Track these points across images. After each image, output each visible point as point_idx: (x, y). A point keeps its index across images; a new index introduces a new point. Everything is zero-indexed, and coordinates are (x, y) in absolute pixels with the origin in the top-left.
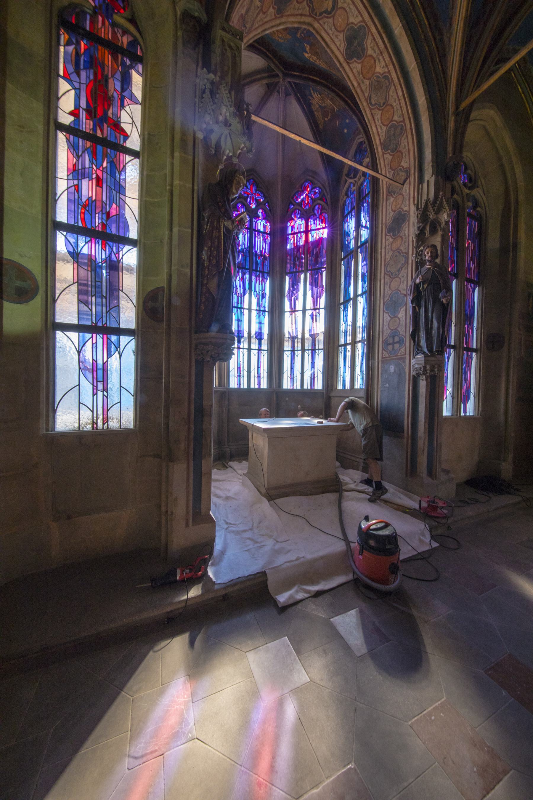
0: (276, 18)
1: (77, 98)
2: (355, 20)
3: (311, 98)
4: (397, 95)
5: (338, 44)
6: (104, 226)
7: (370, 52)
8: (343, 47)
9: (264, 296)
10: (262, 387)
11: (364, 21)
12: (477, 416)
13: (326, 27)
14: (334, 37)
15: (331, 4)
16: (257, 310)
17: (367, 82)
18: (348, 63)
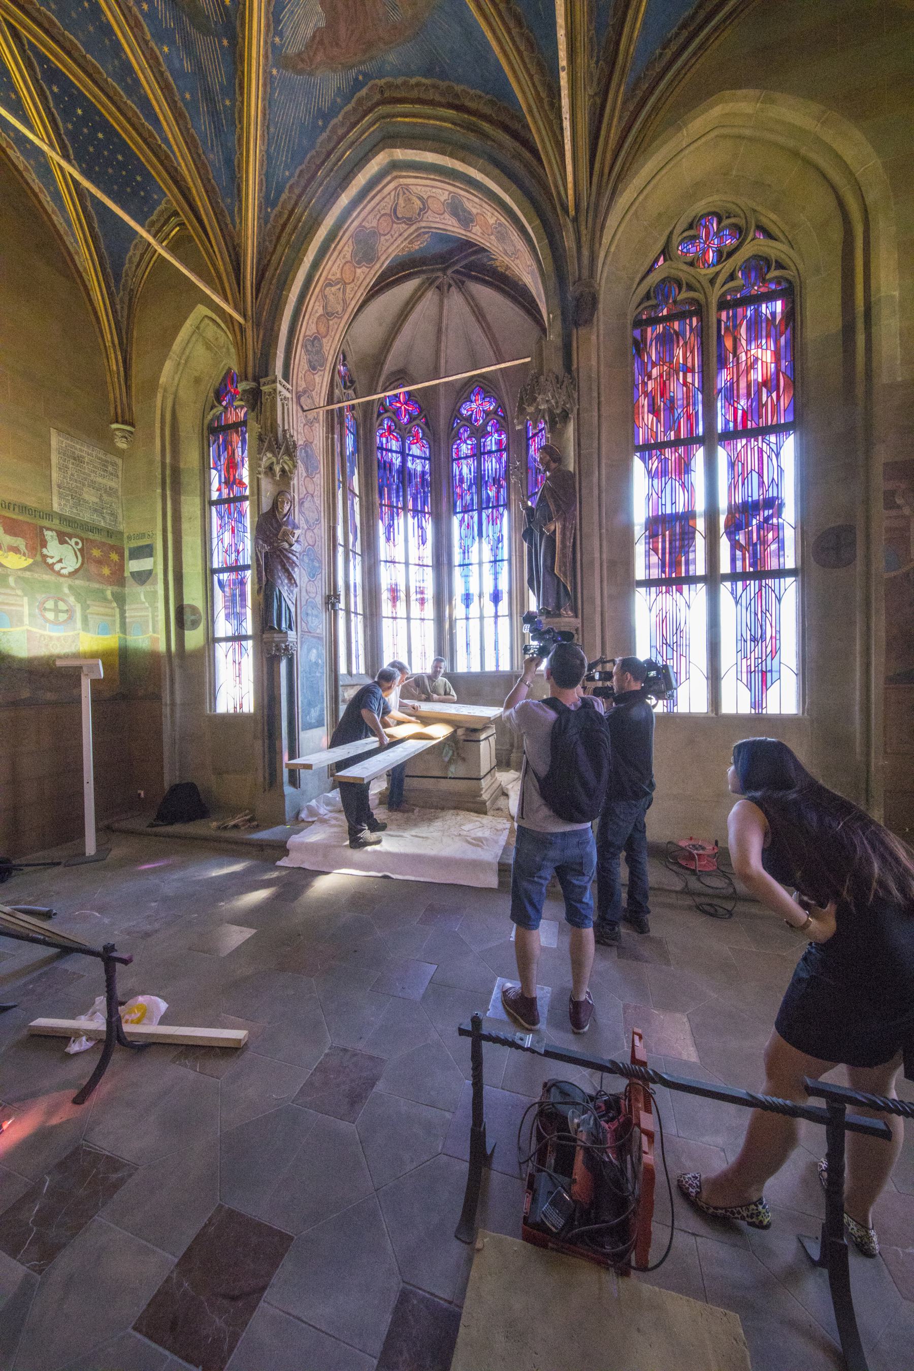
0: (371, 268)
1: (220, 477)
2: (444, 197)
3: (493, 262)
4: (514, 236)
5: (450, 223)
6: (237, 561)
7: (474, 211)
8: (455, 223)
9: (500, 540)
10: (501, 669)
11: (451, 192)
12: (801, 714)
13: (431, 219)
14: (443, 221)
15: (419, 202)
16: (491, 562)
17: (493, 237)
18: (470, 231)
